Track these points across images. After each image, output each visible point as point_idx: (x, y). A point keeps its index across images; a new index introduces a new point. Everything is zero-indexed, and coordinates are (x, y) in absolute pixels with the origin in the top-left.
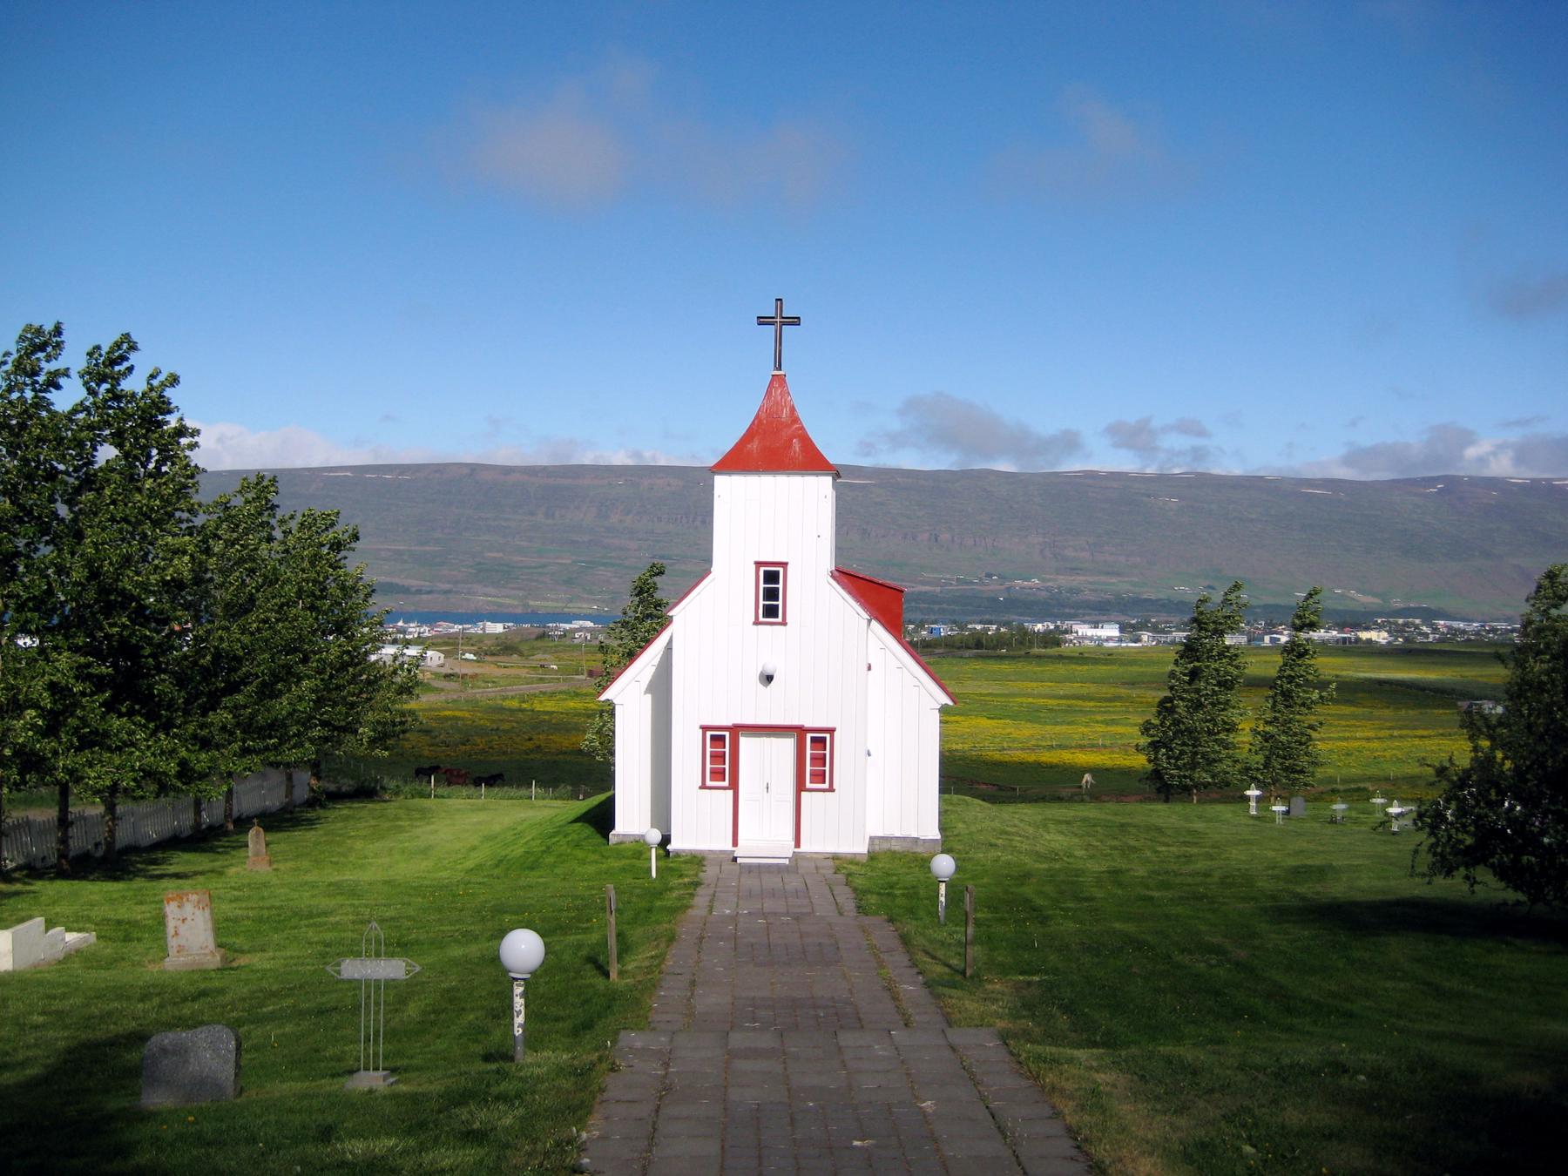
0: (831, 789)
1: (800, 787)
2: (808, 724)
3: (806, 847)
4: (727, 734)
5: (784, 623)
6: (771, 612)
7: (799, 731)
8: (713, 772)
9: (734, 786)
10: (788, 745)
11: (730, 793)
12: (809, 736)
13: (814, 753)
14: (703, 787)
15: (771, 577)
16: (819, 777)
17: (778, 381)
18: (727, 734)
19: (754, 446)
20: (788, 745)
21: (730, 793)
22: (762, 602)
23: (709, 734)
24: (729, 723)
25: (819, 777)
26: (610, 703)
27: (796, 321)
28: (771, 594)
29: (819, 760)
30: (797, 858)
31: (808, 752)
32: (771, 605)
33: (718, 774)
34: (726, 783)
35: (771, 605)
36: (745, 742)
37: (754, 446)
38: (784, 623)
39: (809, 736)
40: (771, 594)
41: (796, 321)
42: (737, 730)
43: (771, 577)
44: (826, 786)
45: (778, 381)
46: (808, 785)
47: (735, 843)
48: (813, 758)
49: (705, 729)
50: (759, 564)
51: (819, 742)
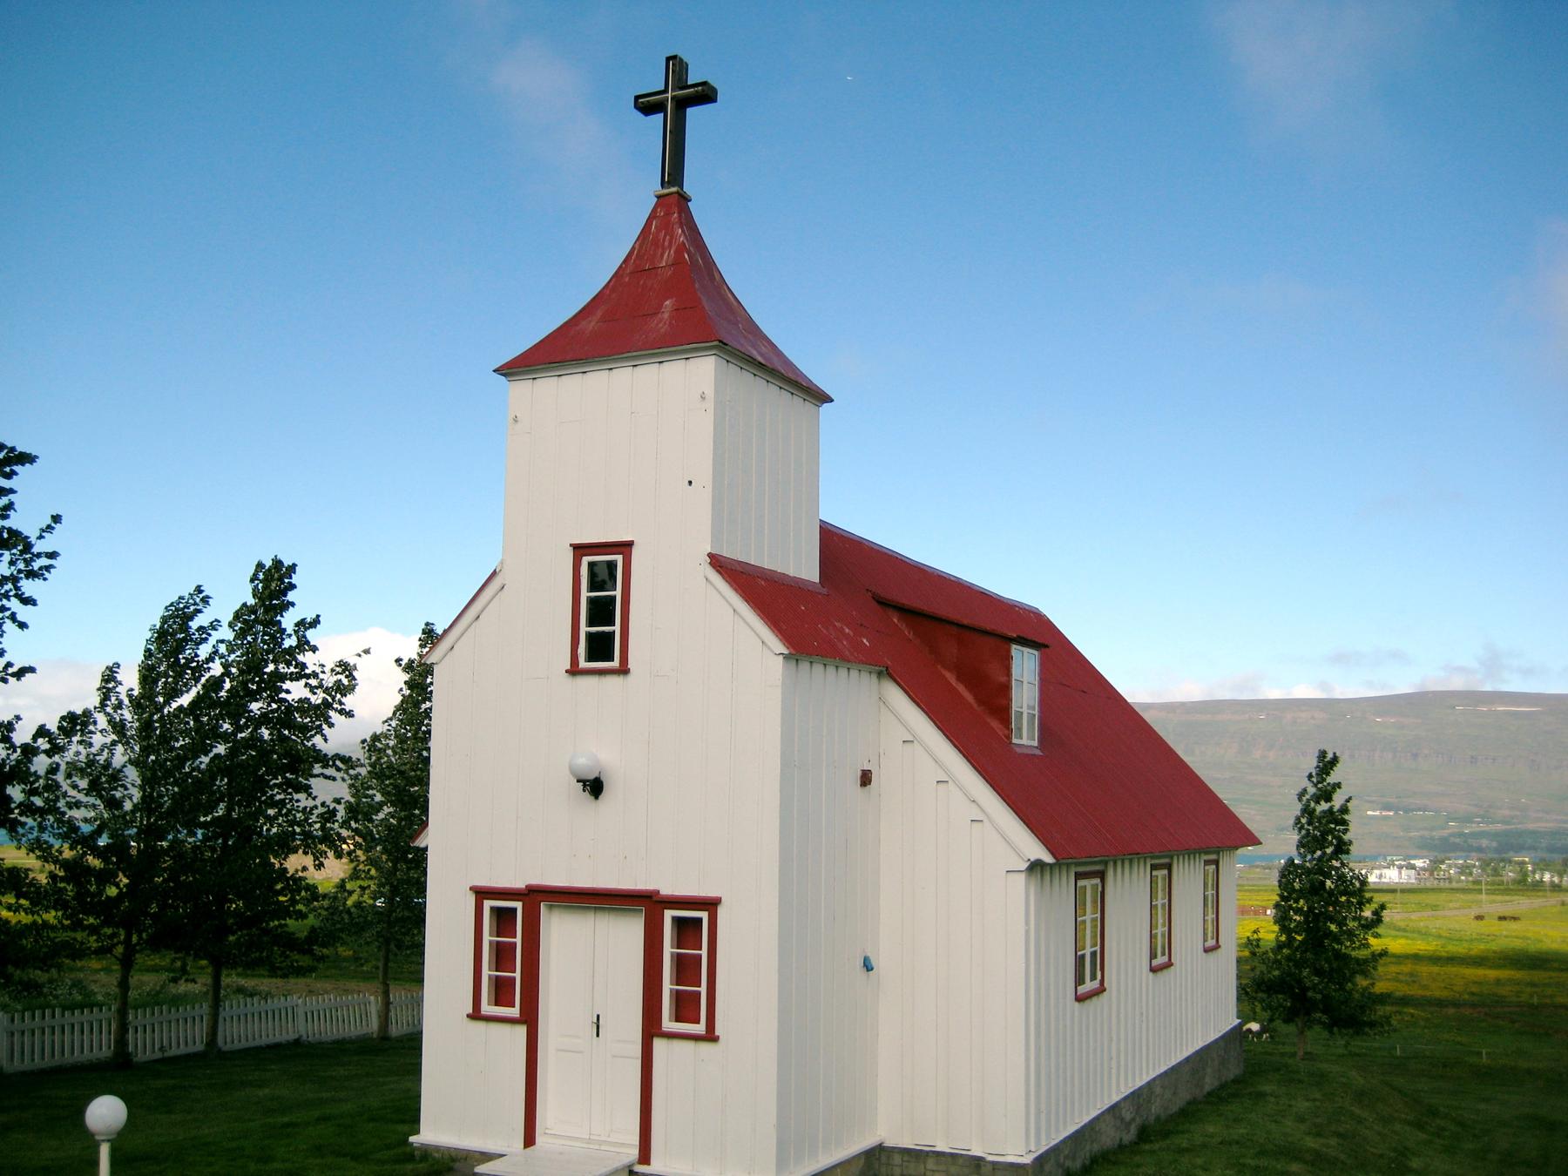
0: (711, 1036)
1: (651, 1029)
2: (667, 889)
4: (518, 905)
5: (624, 670)
6: (600, 648)
7: (649, 904)
9: (530, 1018)
10: (628, 932)
12: (669, 914)
14: (476, 1015)
16: (686, 1008)
17: (673, 204)
18: (518, 905)
20: (628, 932)
21: (521, 1031)
22: (584, 629)
23: (488, 904)
24: (519, 884)
25: (686, 1008)
28: (601, 611)
29: (686, 969)
32: (601, 639)
34: (514, 1012)
35: (601, 639)
37: (591, 325)
38: (624, 670)
39: (669, 914)
41: (706, 95)
42: (535, 896)
44: (700, 1028)
45: (673, 204)
46: (668, 1024)
47: (529, 1140)
49: (481, 894)
50: (580, 550)
51: (687, 930)
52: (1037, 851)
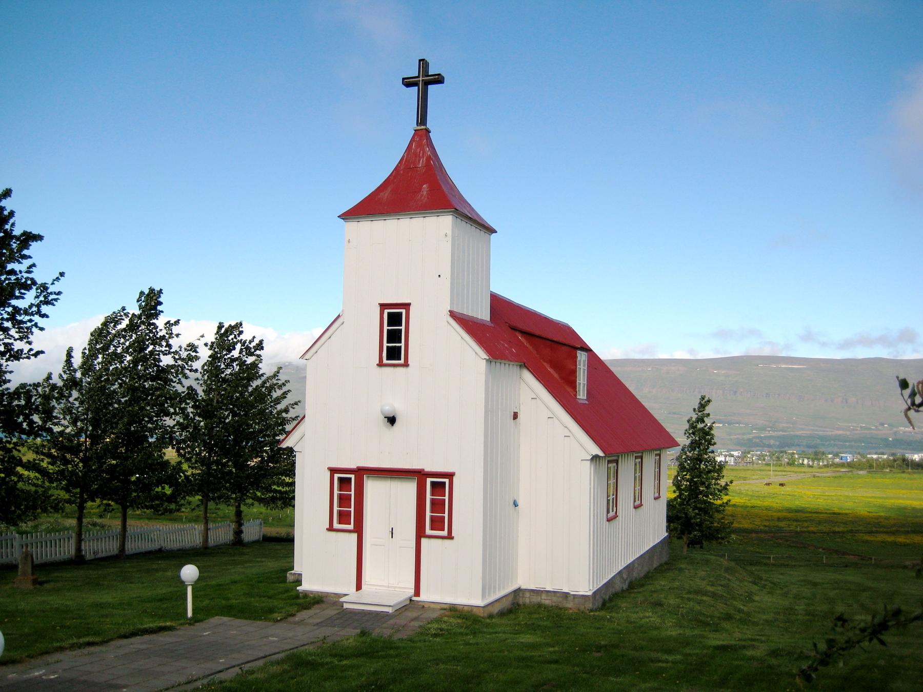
0: (450, 537)
1: (420, 533)
2: (428, 469)
3: (424, 597)
4: (353, 476)
5: (406, 365)
6: (394, 354)
7: (420, 475)
8: (341, 514)
9: (359, 529)
10: (410, 488)
11: (355, 536)
12: (429, 480)
13: (434, 495)
14: (331, 529)
15: (395, 319)
16: (437, 524)
17: (422, 136)
18: (353, 476)
19: (385, 195)
20: (410, 488)
21: (355, 536)
22: (385, 345)
23: (336, 476)
24: (353, 466)
25: (437, 524)
26: (290, 450)
27: (439, 80)
28: (394, 336)
29: (437, 506)
30: (411, 604)
31: (429, 497)
32: (394, 347)
33: (344, 517)
34: (351, 527)
35: (394, 347)
36: (372, 487)
37: (385, 195)
38: (406, 365)
39: (429, 480)
40: (394, 336)
41: (439, 80)
42: (361, 472)
43: (395, 319)
44: (445, 533)
45: (422, 136)
46: (428, 531)
47: (359, 587)
48: (433, 502)
49: (333, 471)
50: (383, 306)
51: (438, 488)
52: (598, 451)
